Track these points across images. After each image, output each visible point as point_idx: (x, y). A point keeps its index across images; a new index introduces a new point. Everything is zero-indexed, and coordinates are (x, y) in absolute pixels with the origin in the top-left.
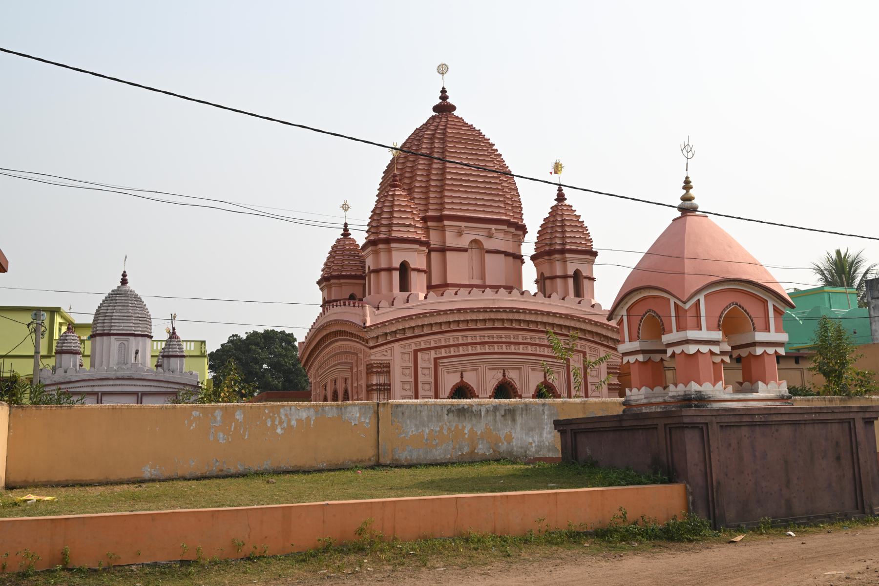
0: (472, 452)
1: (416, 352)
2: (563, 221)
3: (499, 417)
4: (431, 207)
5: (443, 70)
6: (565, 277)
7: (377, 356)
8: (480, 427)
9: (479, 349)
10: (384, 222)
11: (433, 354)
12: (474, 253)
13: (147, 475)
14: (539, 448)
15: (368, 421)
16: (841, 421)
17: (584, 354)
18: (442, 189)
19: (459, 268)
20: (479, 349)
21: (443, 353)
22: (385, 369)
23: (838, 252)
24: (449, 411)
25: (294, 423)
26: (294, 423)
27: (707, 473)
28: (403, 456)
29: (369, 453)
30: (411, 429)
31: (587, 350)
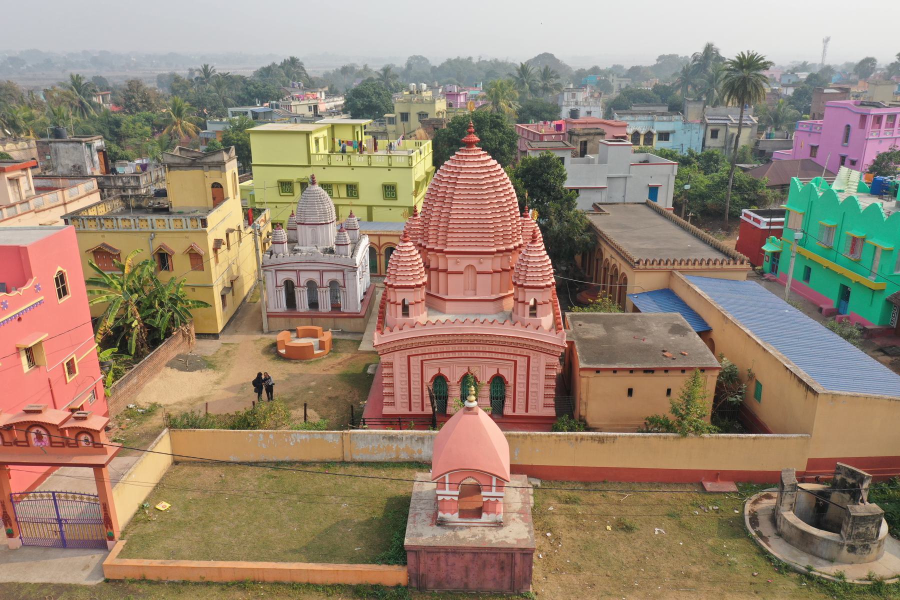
1: (409, 357)
2: (528, 262)
3: (414, 441)
8: (402, 446)
9: (451, 355)
11: (420, 358)
12: (470, 274)
13: (232, 459)
15: (337, 441)
16: (507, 554)
17: (529, 358)
19: (455, 287)
21: (427, 357)
22: (390, 365)
24: (384, 438)
27: (417, 569)
28: (358, 457)
29: (338, 456)
30: (362, 445)
31: (531, 355)
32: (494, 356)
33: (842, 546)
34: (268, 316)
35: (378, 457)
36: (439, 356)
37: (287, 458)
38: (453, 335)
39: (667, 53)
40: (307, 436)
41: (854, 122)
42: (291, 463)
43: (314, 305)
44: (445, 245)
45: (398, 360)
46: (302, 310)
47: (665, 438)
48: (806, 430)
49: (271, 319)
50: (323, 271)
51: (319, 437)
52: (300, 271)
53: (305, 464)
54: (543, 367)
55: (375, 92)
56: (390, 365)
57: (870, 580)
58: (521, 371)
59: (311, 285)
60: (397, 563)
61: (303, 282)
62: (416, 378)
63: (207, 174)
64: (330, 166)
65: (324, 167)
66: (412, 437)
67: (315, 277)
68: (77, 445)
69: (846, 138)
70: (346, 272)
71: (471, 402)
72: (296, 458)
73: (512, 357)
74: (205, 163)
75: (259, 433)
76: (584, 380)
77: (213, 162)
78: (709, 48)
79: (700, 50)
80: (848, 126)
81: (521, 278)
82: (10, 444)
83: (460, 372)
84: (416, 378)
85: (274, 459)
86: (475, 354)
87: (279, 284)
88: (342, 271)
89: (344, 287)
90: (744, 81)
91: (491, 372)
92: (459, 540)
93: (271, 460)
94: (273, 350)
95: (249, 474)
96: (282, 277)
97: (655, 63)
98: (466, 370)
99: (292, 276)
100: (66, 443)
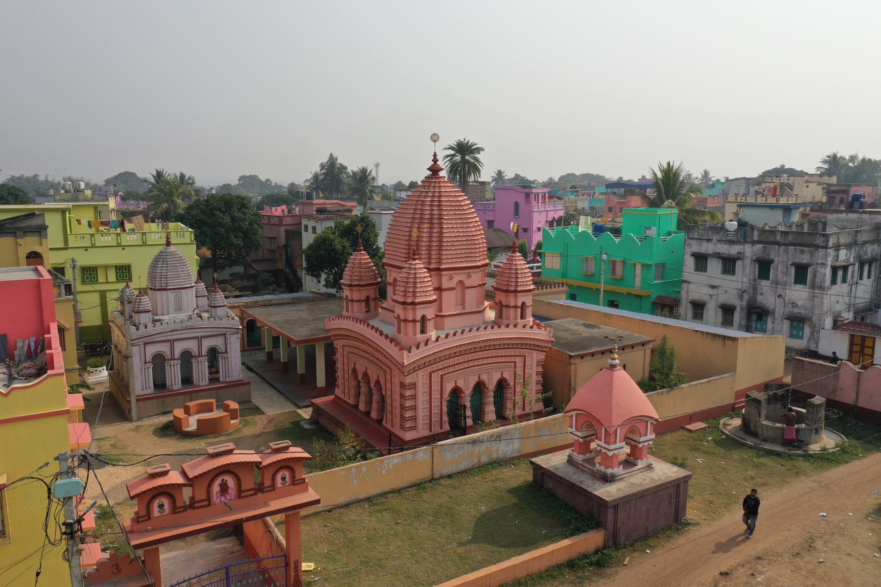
0: (479, 462)
4: (433, 261)
5: (435, 138)
6: (516, 307)
7: (408, 380)
8: (483, 447)
9: (466, 365)
10: (411, 290)
11: (440, 373)
14: (512, 452)
15: (428, 457)
17: (525, 356)
18: (440, 249)
20: (466, 365)
22: (414, 386)
23: (669, 164)
25: (391, 467)
26: (391, 467)
28: (446, 471)
29: (427, 474)
32: (500, 360)
33: (811, 431)
34: (138, 400)
35: (463, 466)
36: (456, 368)
37: (379, 491)
38: (472, 343)
39: (247, 174)
40: (400, 460)
41: (521, 199)
42: (384, 494)
43: (187, 380)
44: (440, 263)
45: (421, 378)
46: (175, 388)
47: (662, 393)
48: (731, 368)
49: (141, 403)
50: (202, 337)
51: (409, 457)
52: (175, 340)
53: (398, 491)
54: (535, 364)
55: (9, 194)
56: (414, 386)
57: (837, 447)
58: (519, 372)
59: (187, 358)
60: (593, 528)
61: (177, 354)
62: (436, 396)
63: (20, 241)
64: (93, 246)
65: (86, 249)
66: (492, 436)
67: (192, 346)
68: (273, 486)
69: (517, 212)
70: (228, 336)
71: (614, 359)
72: (387, 489)
73: (512, 359)
74: (19, 229)
75: (351, 467)
76: (573, 367)
77: (30, 227)
78: (332, 160)
79: (325, 159)
80: (517, 204)
81: (513, 284)
82: (185, 508)
83: (473, 381)
84: (436, 396)
85: (366, 496)
86: (485, 361)
87: (148, 360)
88: (224, 335)
89: (226, 352)
90: (464, 161)
91: (496, 377)
92: (638, 486)
93: (362, 497)
94: (172, 430)
95: (352, 515)
96: (151, 350)
97: (238, 182)
98: (477, 379)
99: (164, 349)
100: (260, 489)
